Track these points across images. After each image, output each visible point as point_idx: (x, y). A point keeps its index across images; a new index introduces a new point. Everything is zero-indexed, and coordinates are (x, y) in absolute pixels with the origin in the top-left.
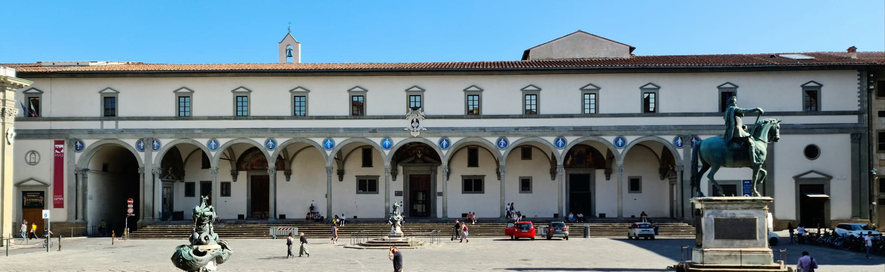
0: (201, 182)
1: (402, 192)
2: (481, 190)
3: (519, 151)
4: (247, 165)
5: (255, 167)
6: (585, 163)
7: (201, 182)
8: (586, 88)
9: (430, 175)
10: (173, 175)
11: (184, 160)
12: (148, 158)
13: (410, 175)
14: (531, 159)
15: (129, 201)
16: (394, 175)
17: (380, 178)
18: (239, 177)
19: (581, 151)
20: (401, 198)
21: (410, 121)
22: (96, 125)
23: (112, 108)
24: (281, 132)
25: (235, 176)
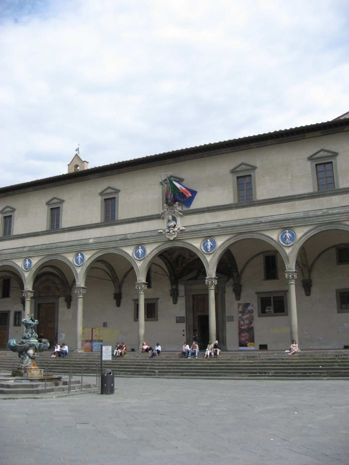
1: (184, 317)
3: (333, 253)
5: (41, 295)
13: (193, 296)
16: (175, 295)
17: (159, 301)
20: (183, 326)
21: (166, 221)
24: (33, 251)
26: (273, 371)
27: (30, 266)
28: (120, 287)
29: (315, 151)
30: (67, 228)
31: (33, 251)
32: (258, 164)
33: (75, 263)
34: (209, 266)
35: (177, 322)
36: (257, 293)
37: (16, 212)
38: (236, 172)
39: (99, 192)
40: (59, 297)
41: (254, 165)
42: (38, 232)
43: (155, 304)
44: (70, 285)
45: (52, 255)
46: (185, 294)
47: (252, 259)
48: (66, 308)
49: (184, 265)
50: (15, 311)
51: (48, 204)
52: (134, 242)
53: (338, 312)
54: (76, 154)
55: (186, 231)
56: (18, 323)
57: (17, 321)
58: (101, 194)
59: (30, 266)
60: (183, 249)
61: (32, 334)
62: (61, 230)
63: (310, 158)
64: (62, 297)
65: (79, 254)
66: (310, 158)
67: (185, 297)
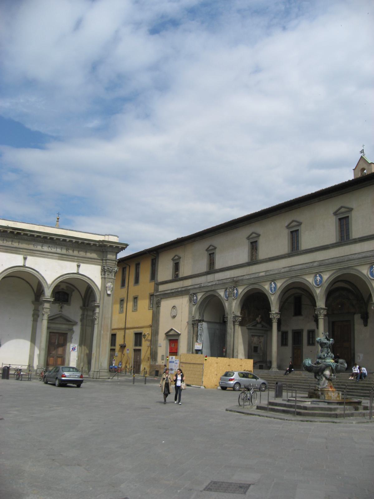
0: (293, 330)
7: (293, 330)
12: (230, 305)
24: (324, 265)
27: (321, 281)
30: (359, 238)
31: (324, 265)
33: (370, 276)
37: (302, 226)
40: (355, 313)
42: (328, 245)
45: (345, 269)
48: (363, 326)
51: (335, 214)
54: (362, 157)
57: (311, 340)
59: (321, 281)
61: (328, 354)
62: (352, 241)
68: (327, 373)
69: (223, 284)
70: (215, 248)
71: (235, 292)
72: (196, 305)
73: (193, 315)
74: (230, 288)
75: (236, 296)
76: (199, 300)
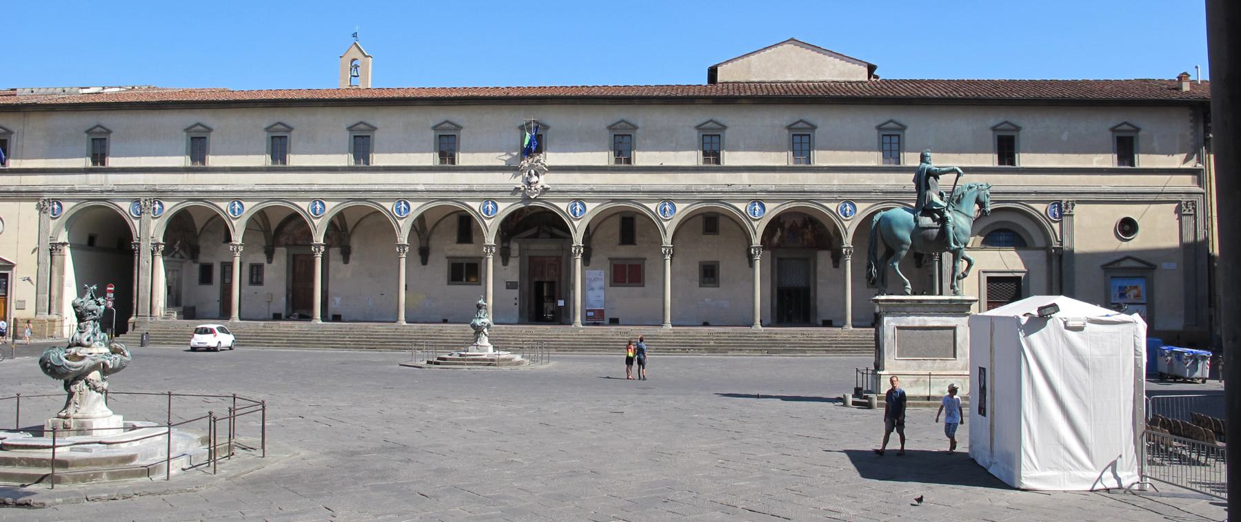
2: (640, 282)
3: (700, 220)
4: (288, 239)
5: (299, 242)
6: (801, 242)
8: (795, 126)
9: (560, 257)
10: (182, 253)
11: (198, 231)
14: (718, 234)
15: (109, 289)
18: (275, 256)
19: (794, 221)
22: (77, 181)
23: (101, 154)
25: (270, 256)
26: (654, 347)
28: (428, 240)
29: (704, 120)
30: (384, 167)
32: (640, 124)
34: (576, 232)
35: (508, 288)
36: (610, 259)
38: (614, 129)
39: (432, 125)
41: (633, 122)
43: (477, 264)
44: (349, 232)
46: (520, 254)
47: (604, 220)
49: (520, 219)
50: (250, 264)
51: (350, 129)
52: (482, 195)
53: (700, 286)
55: (550, 190)
56: (257, 281)
57: (255, 277)
58: (435, 128)
60: (545, 211)
63: (698, 127)
64: (335, 247)
65: (403, 202)
66: (698, 127)
67: (518, 258)
68: (485, 330)
69: (134, 196)
70: (109, 132)
71: (157, 208)
72: (57, 220)
73: (50, 235)
74: (146, 200)
75: (158, 214)
76: (66, 213)
